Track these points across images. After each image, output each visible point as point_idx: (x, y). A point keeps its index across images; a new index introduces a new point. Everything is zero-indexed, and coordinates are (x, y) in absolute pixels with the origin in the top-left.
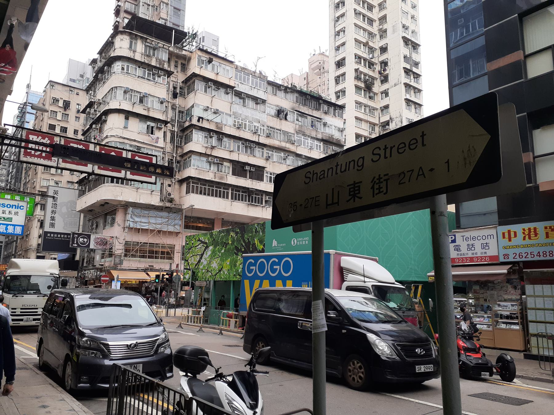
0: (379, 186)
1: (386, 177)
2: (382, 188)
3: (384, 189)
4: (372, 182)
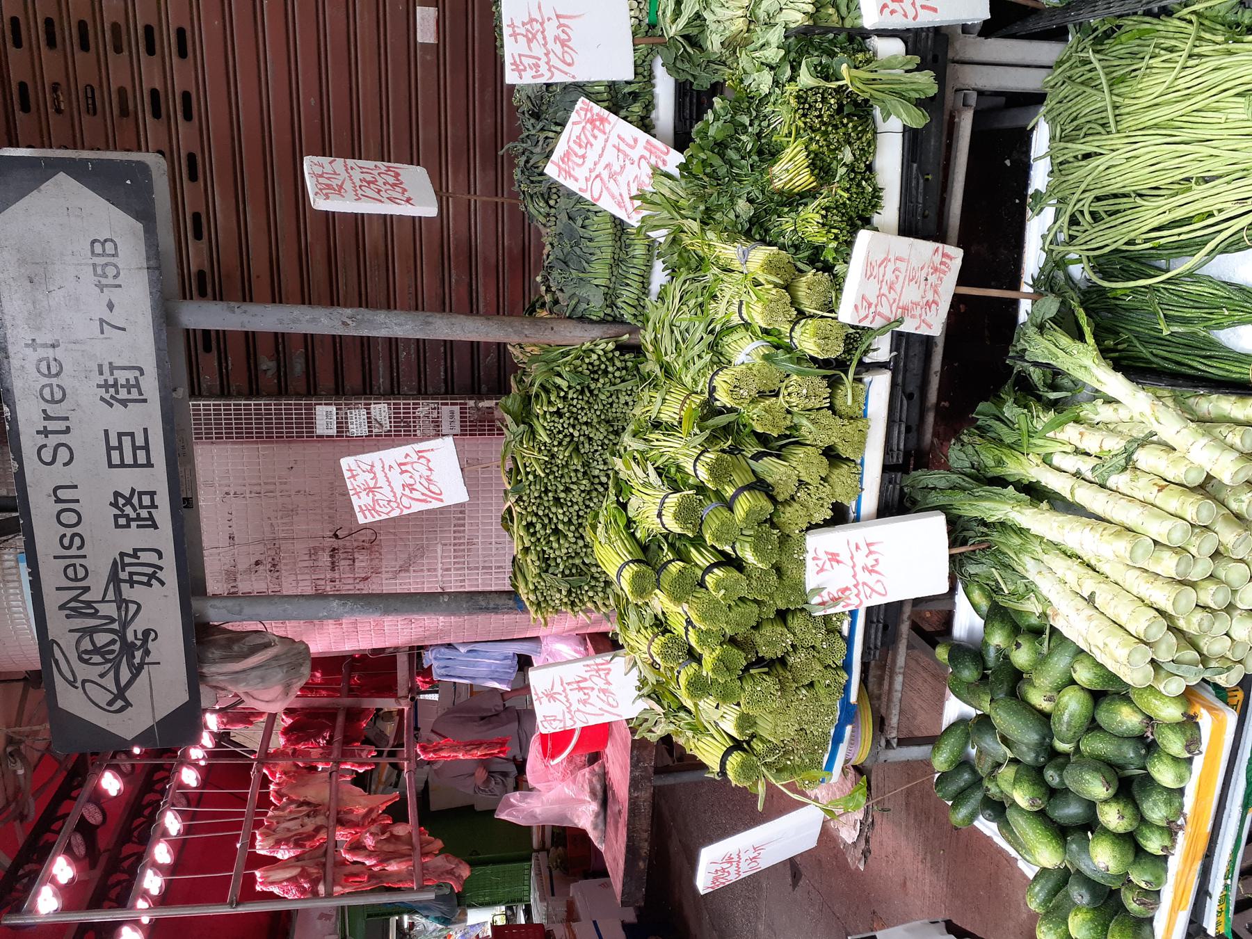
0: (122, 386)
2: (128, 380)
3: (131, 375)
4: (111, 405)
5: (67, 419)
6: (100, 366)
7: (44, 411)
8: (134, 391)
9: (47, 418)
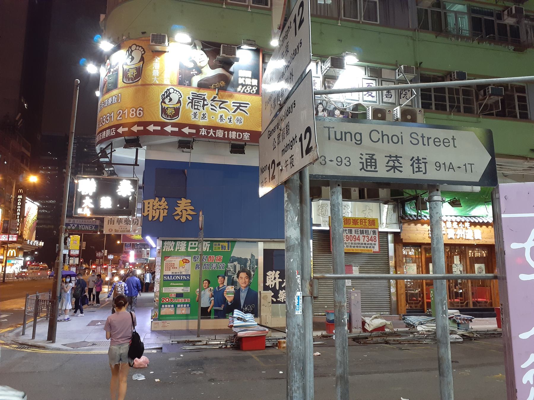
1: (425, 161)
4: (411, 160)
6: (425, 159)
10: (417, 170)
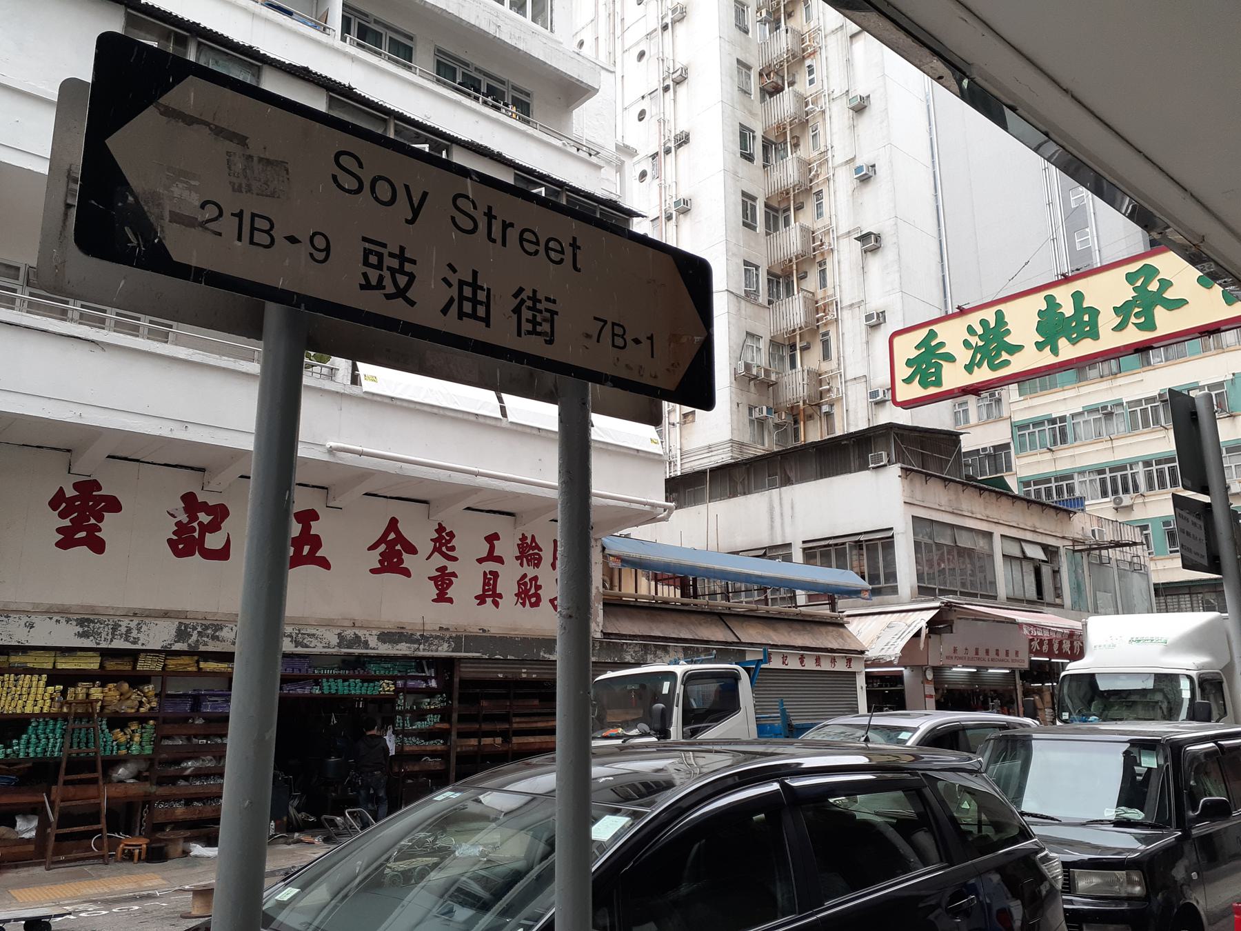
0: (534, 316)
1: (550, 306)
4: (516, 296)
5: (504, 244)
6: (554, 302)
7: (512, 225)
8: (529, 327)
9: (506, 226)
10: (527, 327)
